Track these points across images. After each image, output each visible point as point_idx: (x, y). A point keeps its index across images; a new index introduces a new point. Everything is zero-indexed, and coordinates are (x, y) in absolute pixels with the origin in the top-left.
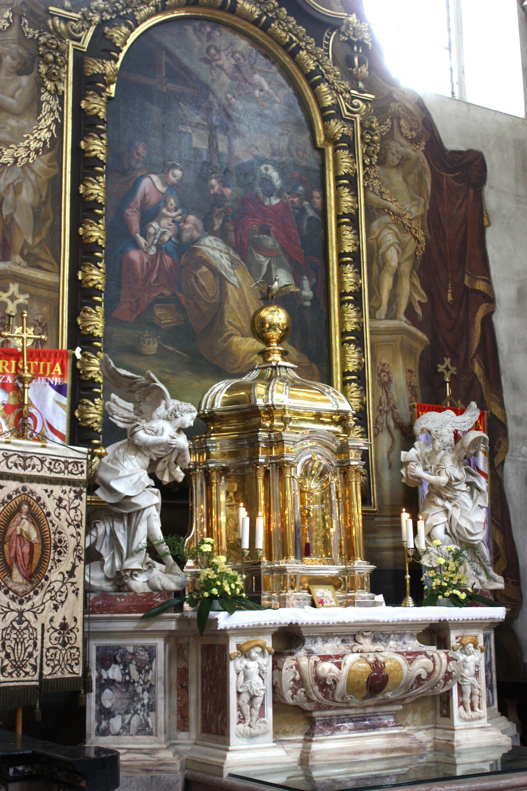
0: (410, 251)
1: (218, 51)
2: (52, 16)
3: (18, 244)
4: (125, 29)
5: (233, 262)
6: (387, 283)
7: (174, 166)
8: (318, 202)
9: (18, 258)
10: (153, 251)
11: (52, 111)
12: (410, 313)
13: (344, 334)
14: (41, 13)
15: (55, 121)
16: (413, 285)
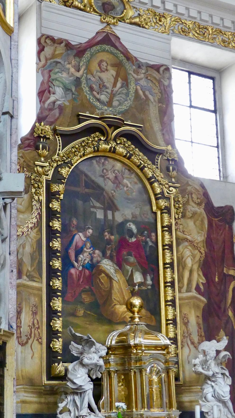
0: (197, 258)
1: (107, 171)
2: (37, 166)
3: (25, 271)
4: (67, 169)
5: (116, 271)
6: (186, 274)
7: (89, 228)
8: (154, 238)
9: (25, 277)
10: (80, 268)
11: (37, 209)
12: (198, 289)
13: (166, 301)
14: (31, 164)
15: (39, 214)
16: (199, 275)
